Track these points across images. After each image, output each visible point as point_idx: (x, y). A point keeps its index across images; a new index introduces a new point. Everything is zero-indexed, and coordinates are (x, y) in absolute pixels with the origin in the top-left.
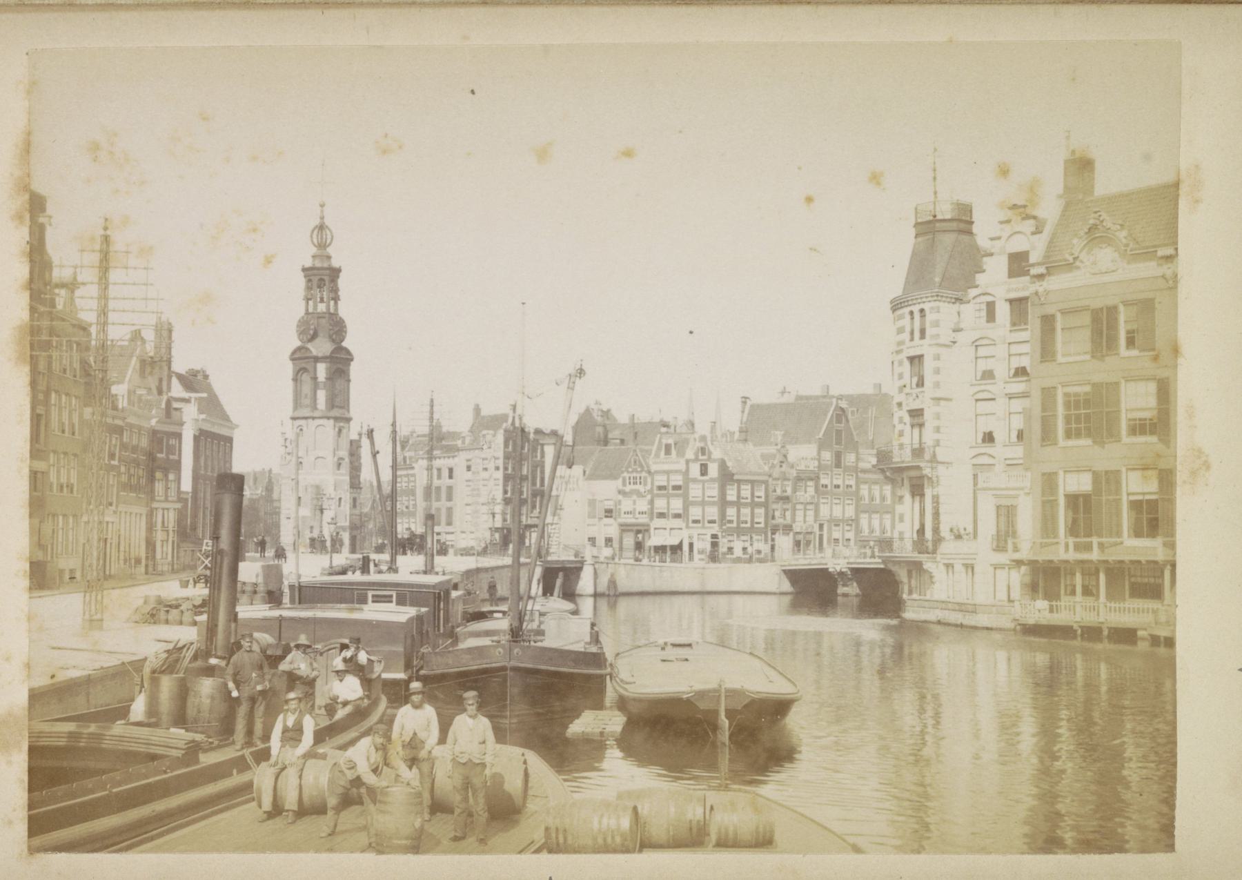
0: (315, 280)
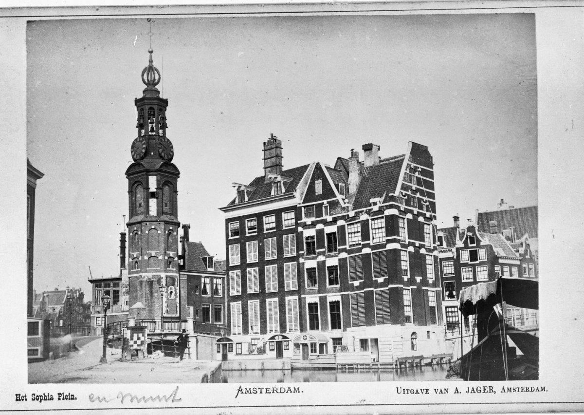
0: (147, 107)
